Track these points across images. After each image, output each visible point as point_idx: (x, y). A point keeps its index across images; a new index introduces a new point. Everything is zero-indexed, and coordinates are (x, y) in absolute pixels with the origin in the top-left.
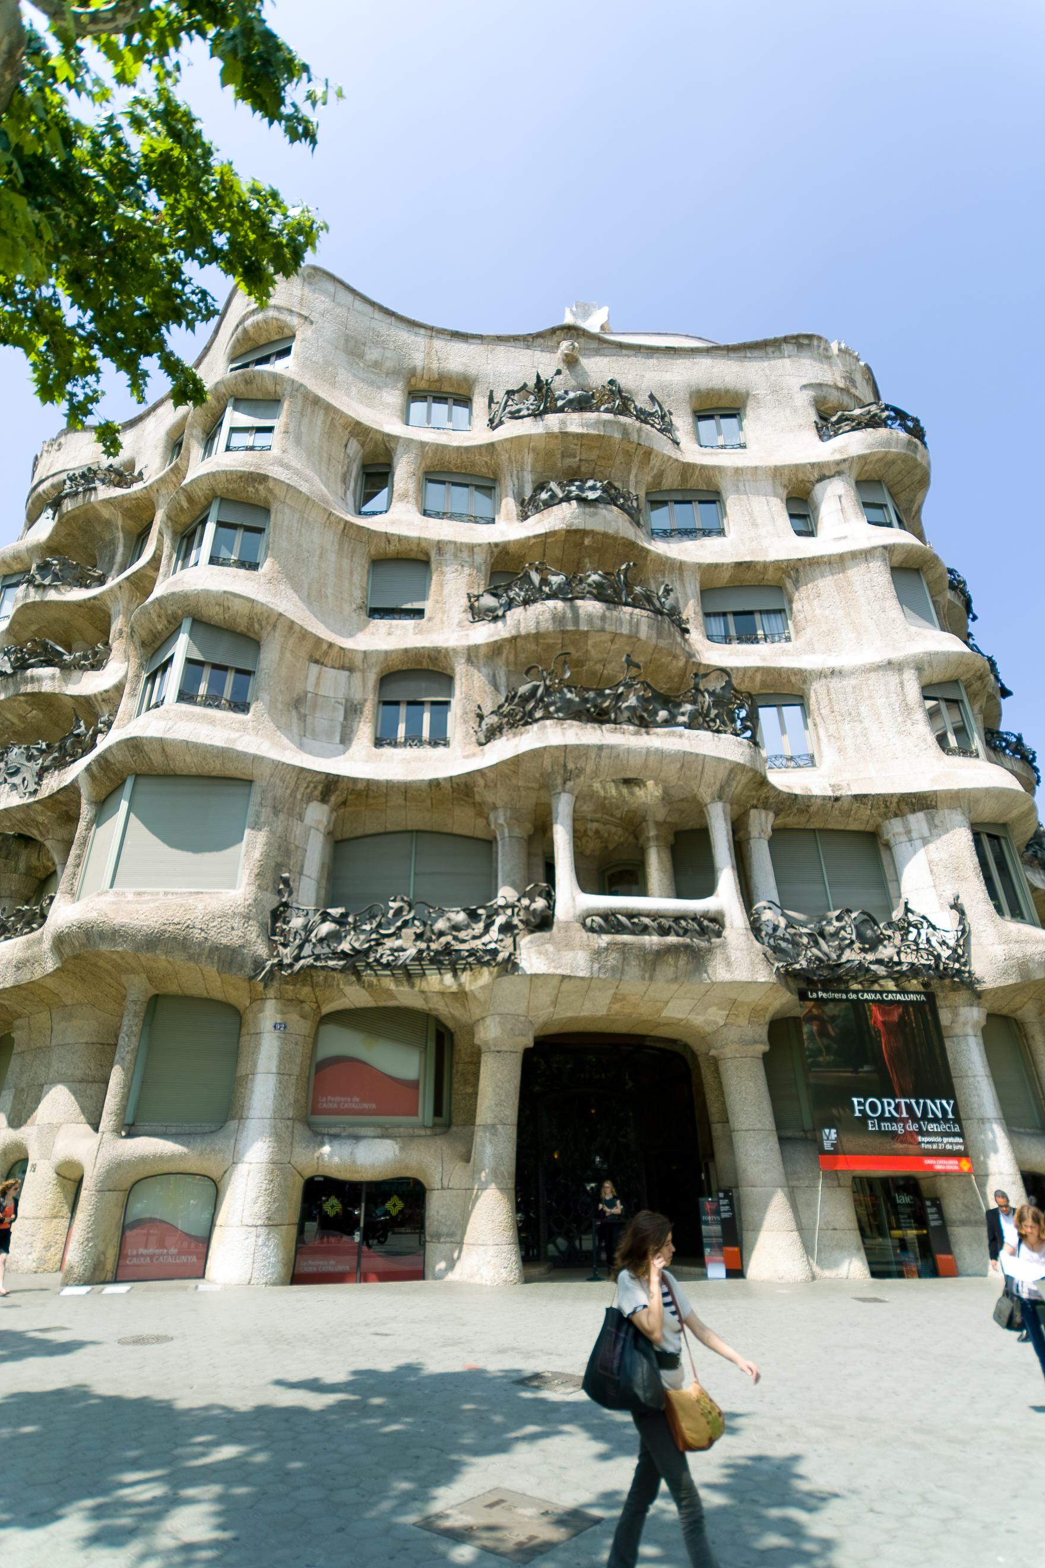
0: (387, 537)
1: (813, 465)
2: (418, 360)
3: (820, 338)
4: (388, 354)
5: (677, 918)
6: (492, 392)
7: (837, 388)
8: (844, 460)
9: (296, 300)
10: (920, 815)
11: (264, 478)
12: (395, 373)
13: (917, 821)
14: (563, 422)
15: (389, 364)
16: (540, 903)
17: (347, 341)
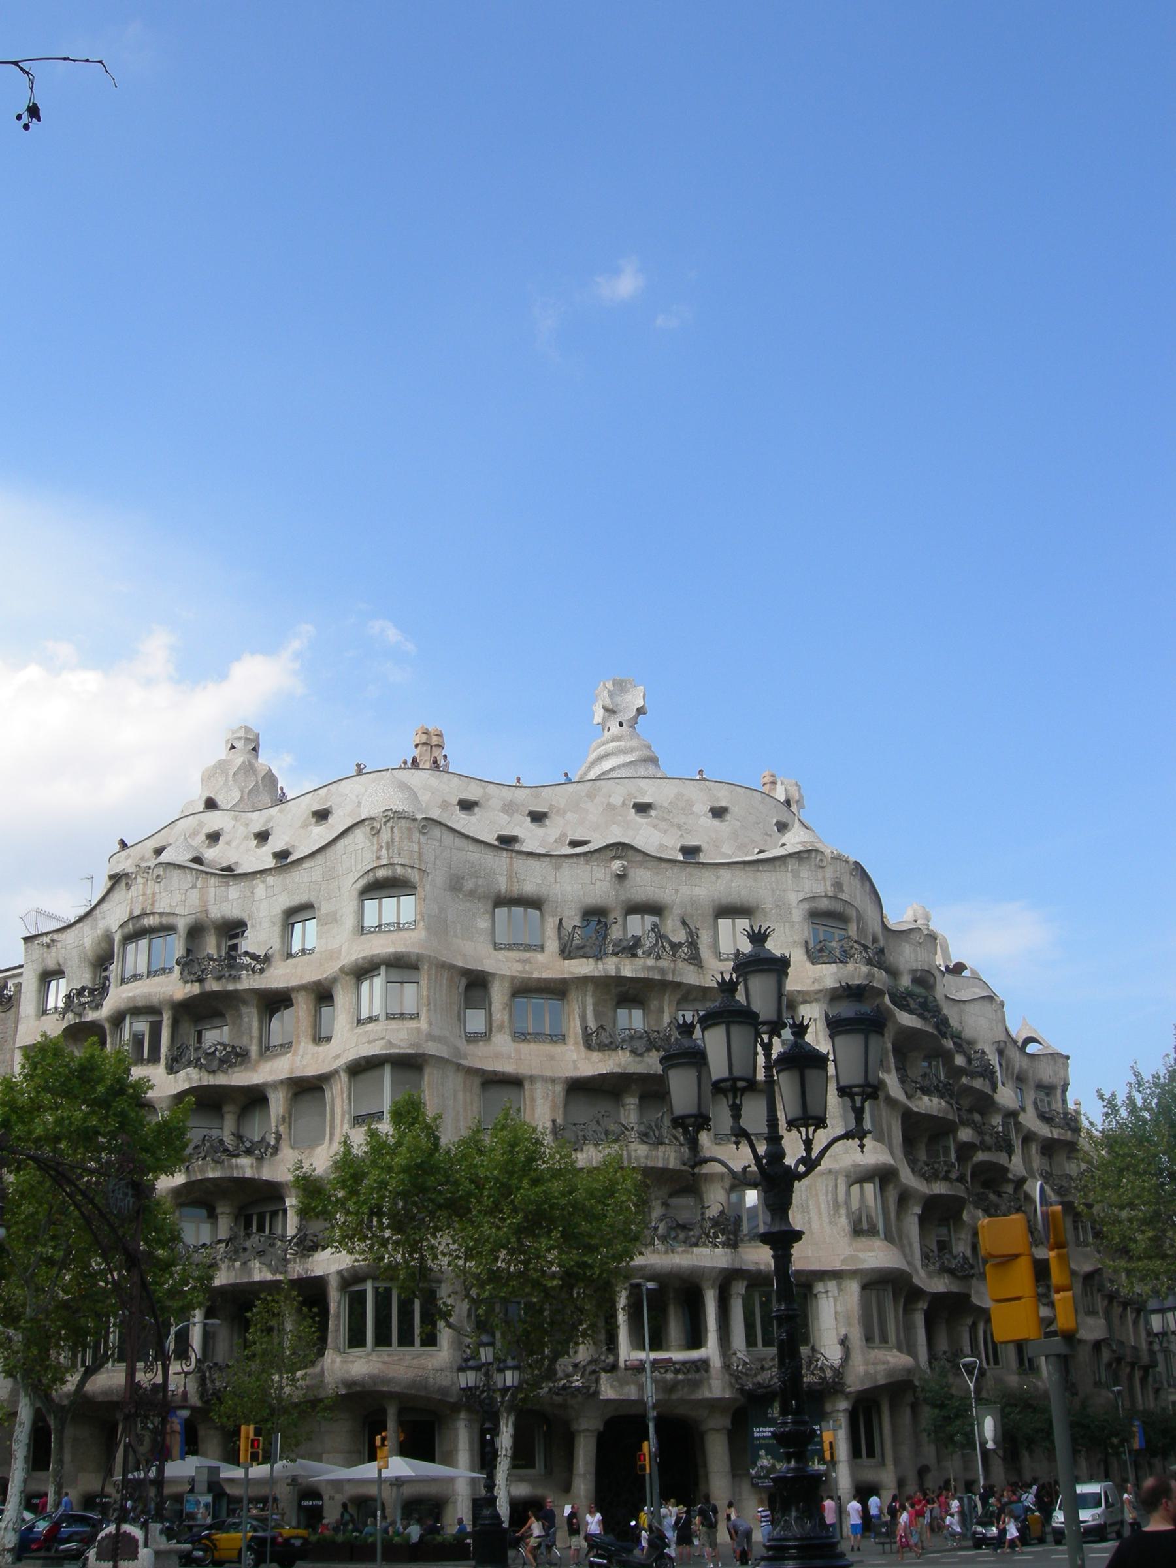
0: (495, 1073)
1: (799, 992)
2: (502, 885)
3: (817, 851)
4: (480, 882)
5: (684, 1363)
6: (561, 920)
7: (826, 896)
8: (821, 991)
9: (416, 856)
10: (834, 1282)
11: (424, 1054)
12: (485, 897)
13: (832, 1285)
14: (618, 969)
15: (481, 890)
16: (611, 1359)
17: (451, 880)
